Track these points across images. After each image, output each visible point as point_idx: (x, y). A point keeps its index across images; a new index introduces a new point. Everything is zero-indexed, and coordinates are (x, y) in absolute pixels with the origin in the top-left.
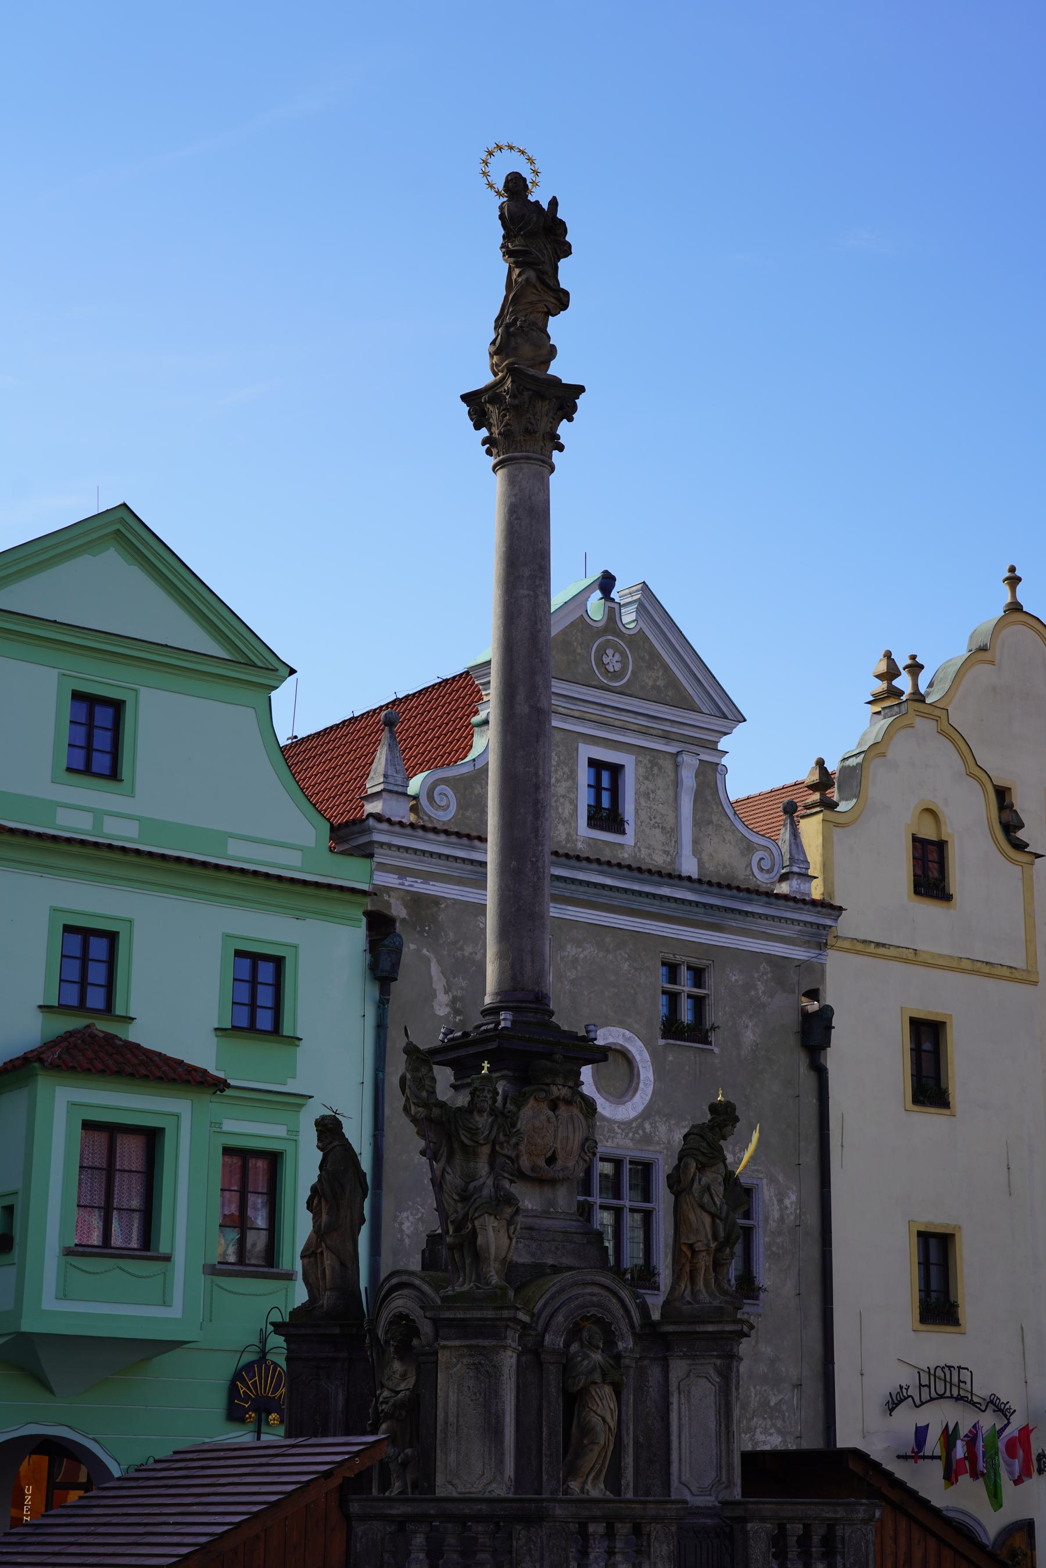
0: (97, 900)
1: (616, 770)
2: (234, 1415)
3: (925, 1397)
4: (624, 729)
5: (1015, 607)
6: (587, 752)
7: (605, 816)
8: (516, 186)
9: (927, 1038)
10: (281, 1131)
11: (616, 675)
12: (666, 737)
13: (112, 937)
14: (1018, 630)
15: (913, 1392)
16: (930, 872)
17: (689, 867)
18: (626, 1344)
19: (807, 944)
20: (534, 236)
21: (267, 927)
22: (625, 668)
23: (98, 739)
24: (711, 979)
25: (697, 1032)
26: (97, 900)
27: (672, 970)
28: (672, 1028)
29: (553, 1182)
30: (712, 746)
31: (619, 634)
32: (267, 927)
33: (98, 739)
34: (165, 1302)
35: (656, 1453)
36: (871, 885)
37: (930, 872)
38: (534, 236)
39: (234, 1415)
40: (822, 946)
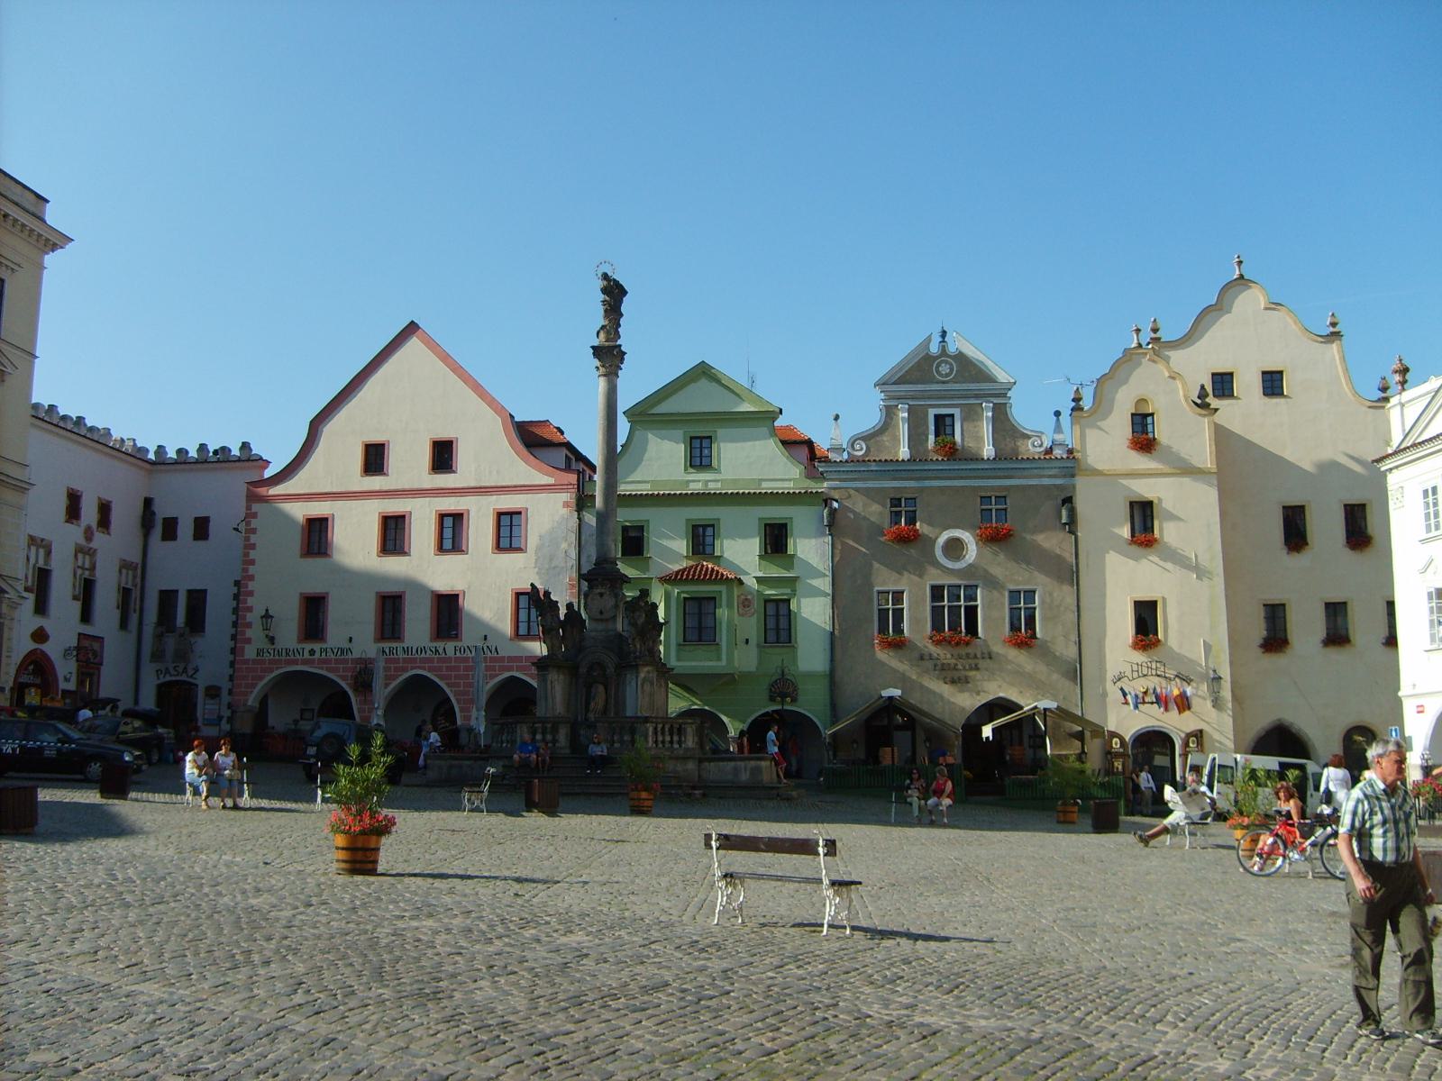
1: (952, 416)
2: (772, 699)
3: (1135, 675)
4: (952, 398)
5: (1241, 277)
6: (932, 412)
8: (605, 277)
10: (788, 591)
11: (947, 375)
12: (977, 396)
13: (713, 526)
15: (1128, 673)
18: (611, 670)
19: (1065, 476)
20: (614, 293)
22: (952, 370)
23: (699, 456)
24: (1008, 501)
29: (607, 620)
30: (1004, 395)
31: (949, 356)
33: (699, 456)
34: (719, 659)
36: (1107, 446)
38: (614, 293)
39: (772, 699)
40: (1073, 476)
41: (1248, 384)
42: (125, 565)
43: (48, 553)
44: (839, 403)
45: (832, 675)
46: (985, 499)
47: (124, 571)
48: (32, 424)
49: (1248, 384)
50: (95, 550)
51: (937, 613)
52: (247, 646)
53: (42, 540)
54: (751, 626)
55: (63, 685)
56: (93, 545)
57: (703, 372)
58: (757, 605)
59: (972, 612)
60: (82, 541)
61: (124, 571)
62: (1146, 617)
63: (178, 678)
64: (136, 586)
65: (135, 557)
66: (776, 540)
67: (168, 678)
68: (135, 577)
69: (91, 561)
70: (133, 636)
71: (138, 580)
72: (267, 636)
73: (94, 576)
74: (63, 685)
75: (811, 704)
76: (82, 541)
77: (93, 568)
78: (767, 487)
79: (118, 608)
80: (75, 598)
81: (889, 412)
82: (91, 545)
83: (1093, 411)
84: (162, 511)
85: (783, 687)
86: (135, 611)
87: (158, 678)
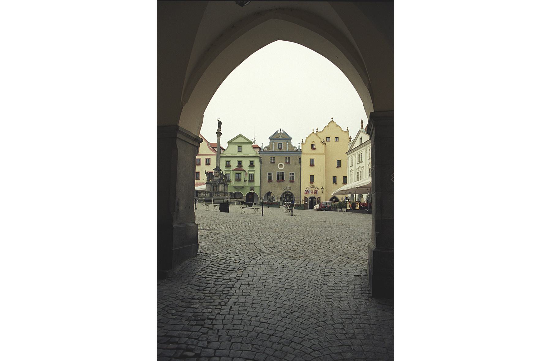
0: (240, 159)
7: (280, 148)
9: (312, 161)
14: (332, 123)
16: (313, 147)
17: (287, 150)
20: (220, 123)
21: (251, 159)
23: (240, 149)
25: (289, 163)
26: (240, 159)
27: (286, 158)
28: (286, 163)
32: (251, 159)
33: (240, 149)
35: (218, 190)
36: (307, 149)
37: (313, 147)
38: (220, 123)
41: (332, 139)
44: (264, 142)
45: (260, 186)
46: (286, 158)
49: (332, 139)
51: (278, 176)
54: (247, 178)
57: (240, 136)
58: (248, 175)
59: (283, 176)
62: (312, 178)
66: (252, 164)
75: (256, 191)
78: (250, 155)
81: (271, 142)
83: (305, 143)
85: (252, 188)
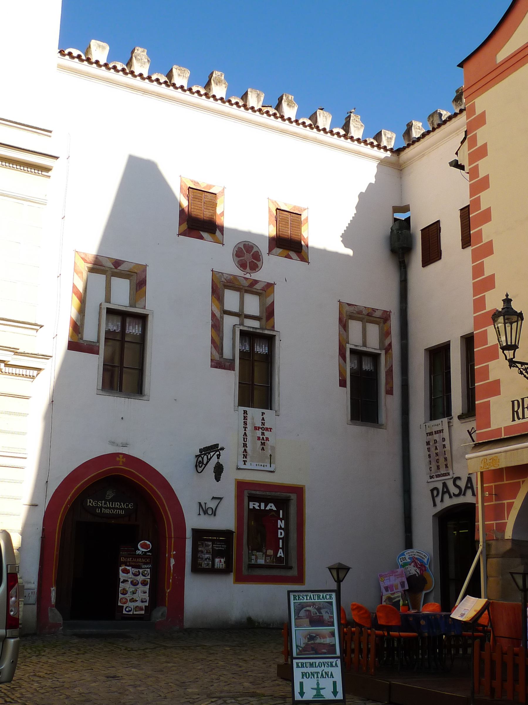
42: (348, 315)
43: (139, 284)
47: (355, 327)
48: (61, 67)
50: (270, 286)
52: (493, 400)
53: (117, 263)
55: (193, 521)
56: (262, 276)
60: (230, 268)
61: (355, 327)
63: (461, 500)
64: (388, 349)
65: (386, 301)
67: (448, 502)
68: (385, 334)
69: (262, 304)
70: (386, 436)
71: (395, 340)
72: (512, 363)
73: (273, 328)
74: (193, 521)
76: (230, 268)
77: (269, 313)
79: (342, 384)
80: (220, 364)
82: (255, 276)
84: (420, 222)
86: (390, 392)
87: (435, 505)
